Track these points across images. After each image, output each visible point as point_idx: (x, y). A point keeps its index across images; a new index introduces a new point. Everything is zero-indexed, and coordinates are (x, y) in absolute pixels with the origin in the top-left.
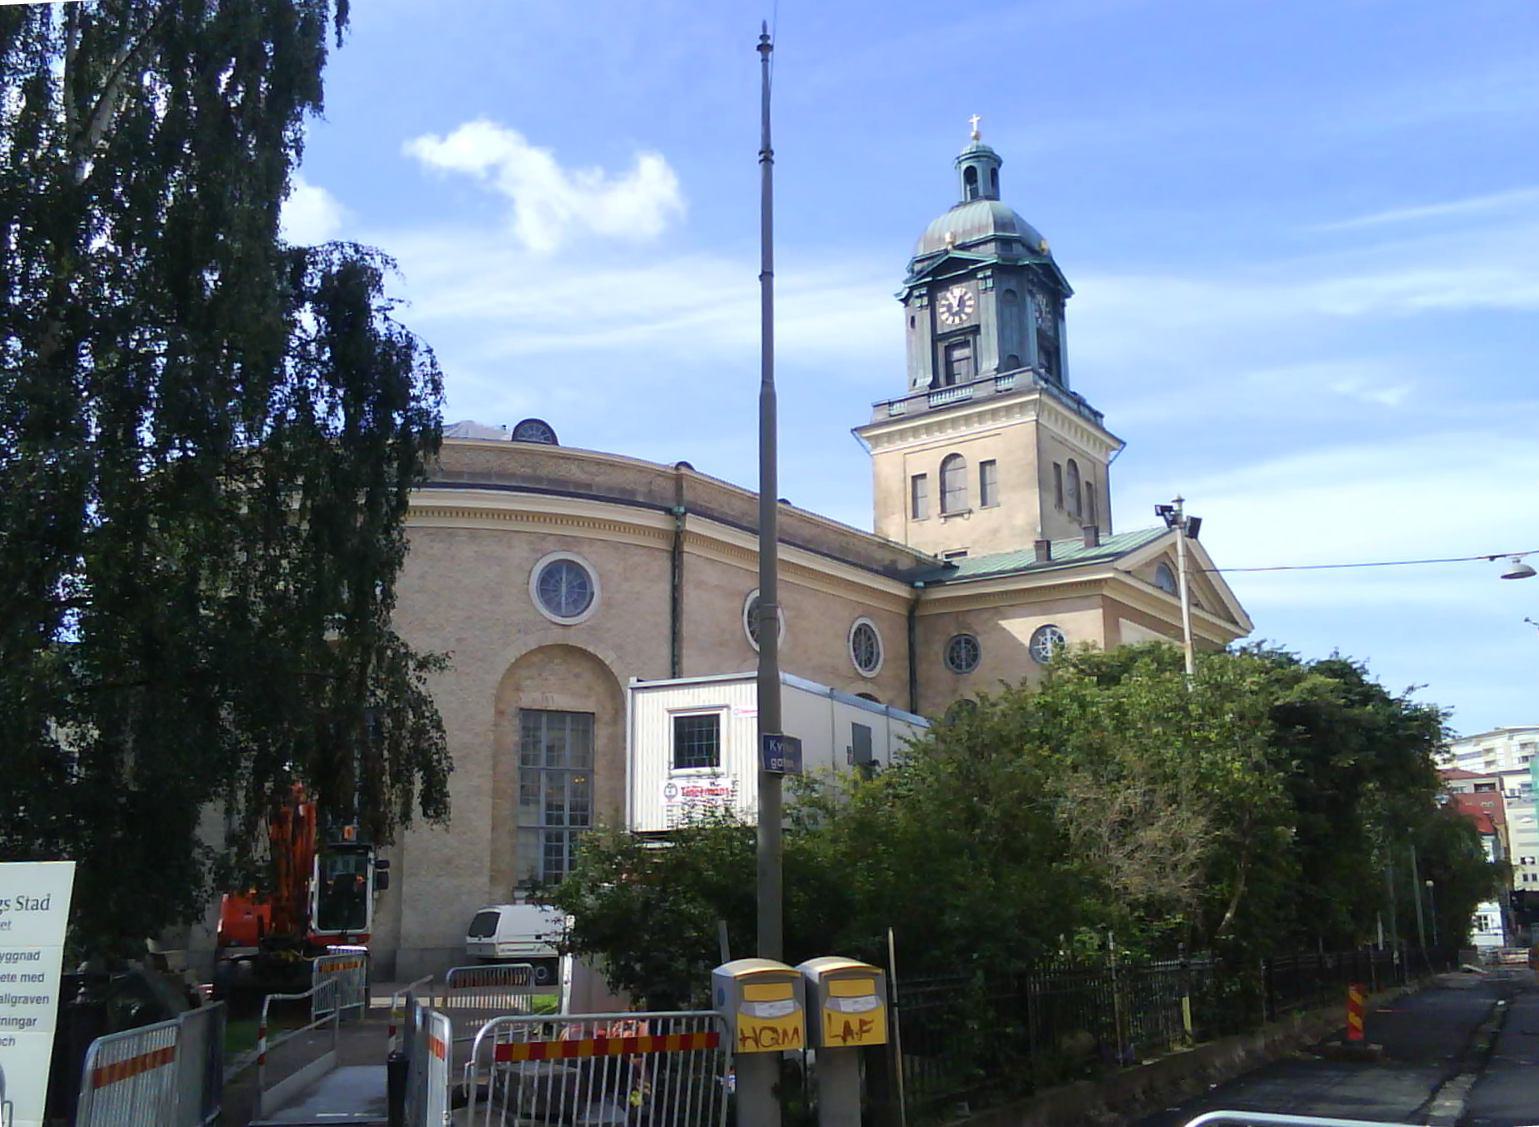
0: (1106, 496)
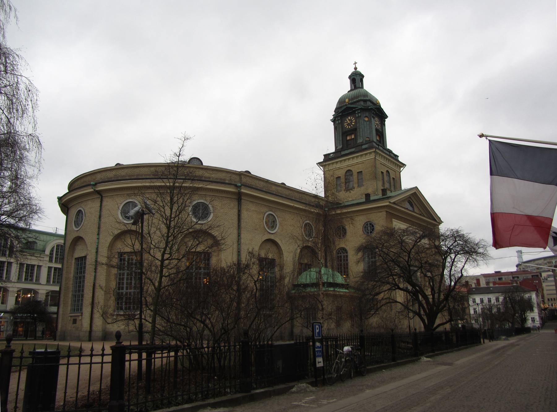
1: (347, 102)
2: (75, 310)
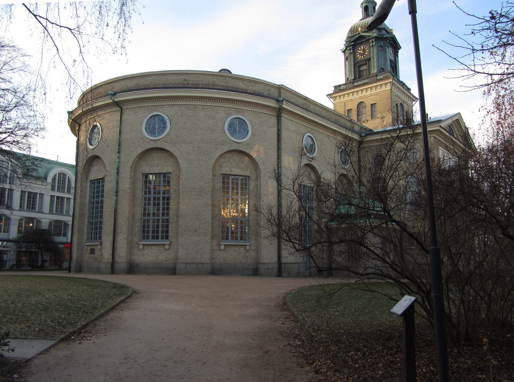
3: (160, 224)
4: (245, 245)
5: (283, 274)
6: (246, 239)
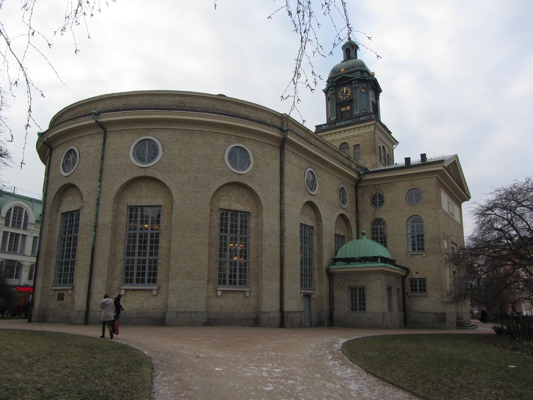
0: (393, 160)
1: (343, 72)
2: (62, 282)
3: (147, 265)
4: (245, 291)
5: (286, 325)
6: (245, 284)
